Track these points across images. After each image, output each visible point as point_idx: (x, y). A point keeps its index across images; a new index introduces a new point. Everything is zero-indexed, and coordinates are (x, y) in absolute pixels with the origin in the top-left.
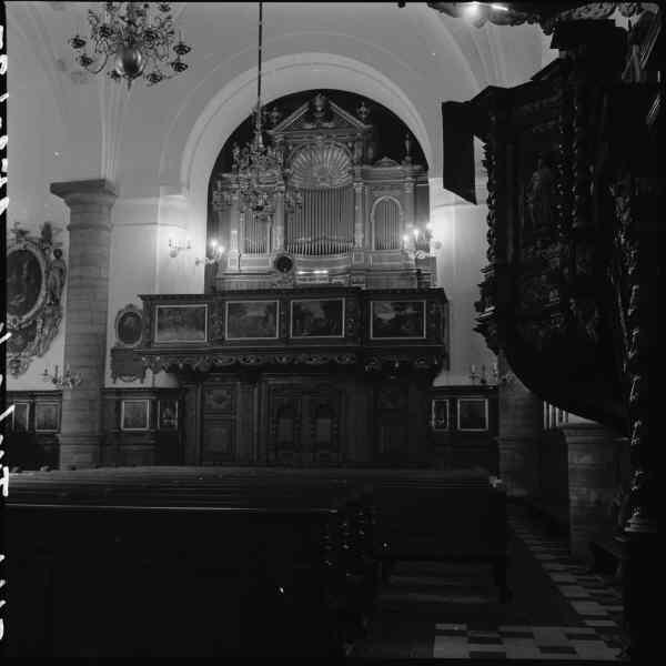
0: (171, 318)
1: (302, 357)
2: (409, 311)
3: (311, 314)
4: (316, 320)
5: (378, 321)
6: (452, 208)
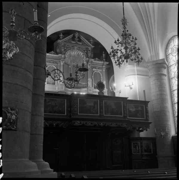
0: (50, 103)
1: (108, 124)
2: (140, 109)
5: (130, 111)
6: (136, 76)
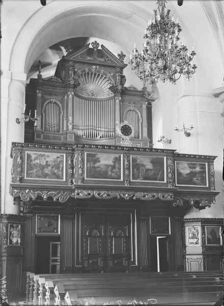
0: (37, 161)
2: (198, 169)
3: (144, 166)
4: (148, 170)
5: (179, 174)
